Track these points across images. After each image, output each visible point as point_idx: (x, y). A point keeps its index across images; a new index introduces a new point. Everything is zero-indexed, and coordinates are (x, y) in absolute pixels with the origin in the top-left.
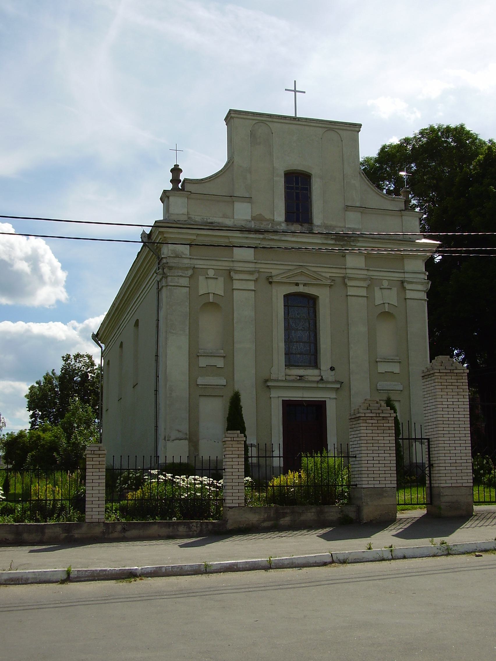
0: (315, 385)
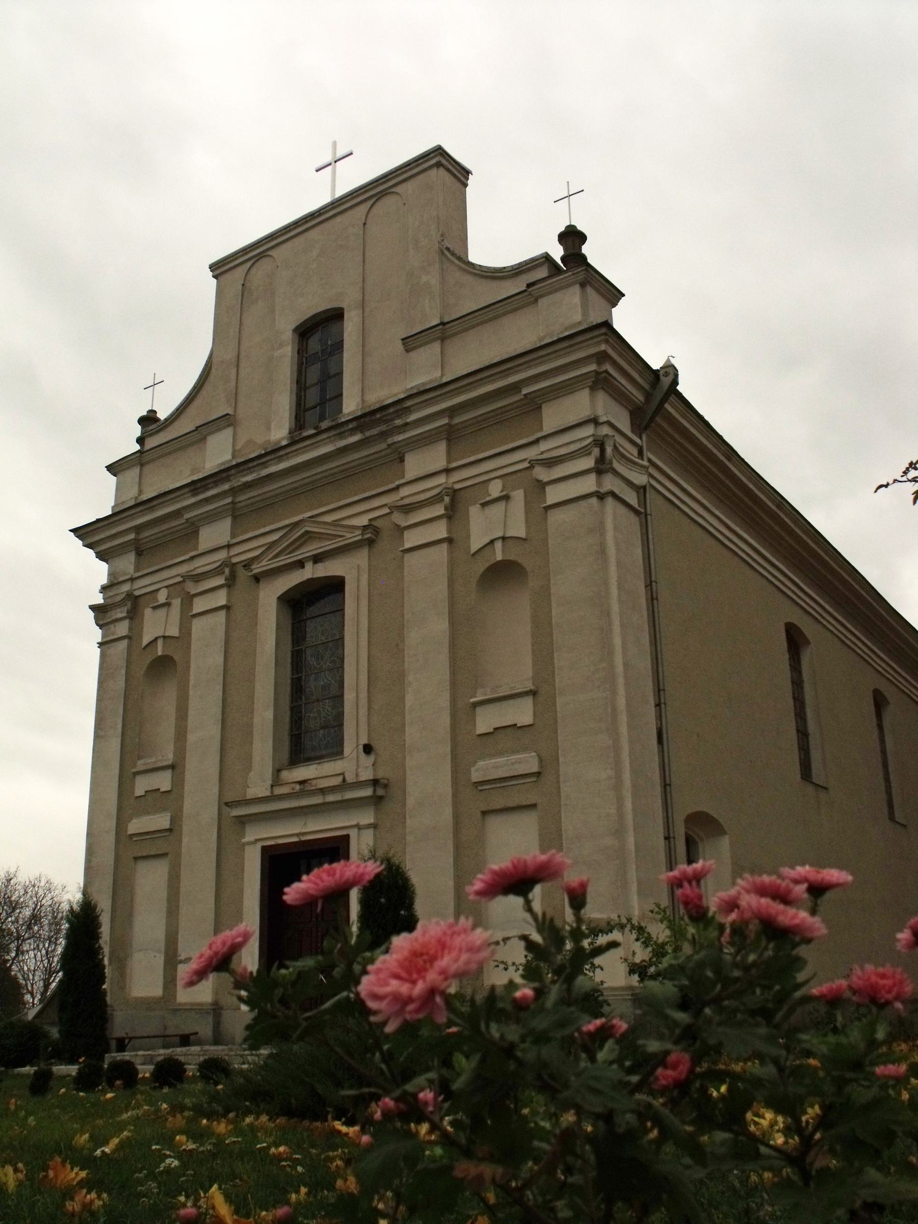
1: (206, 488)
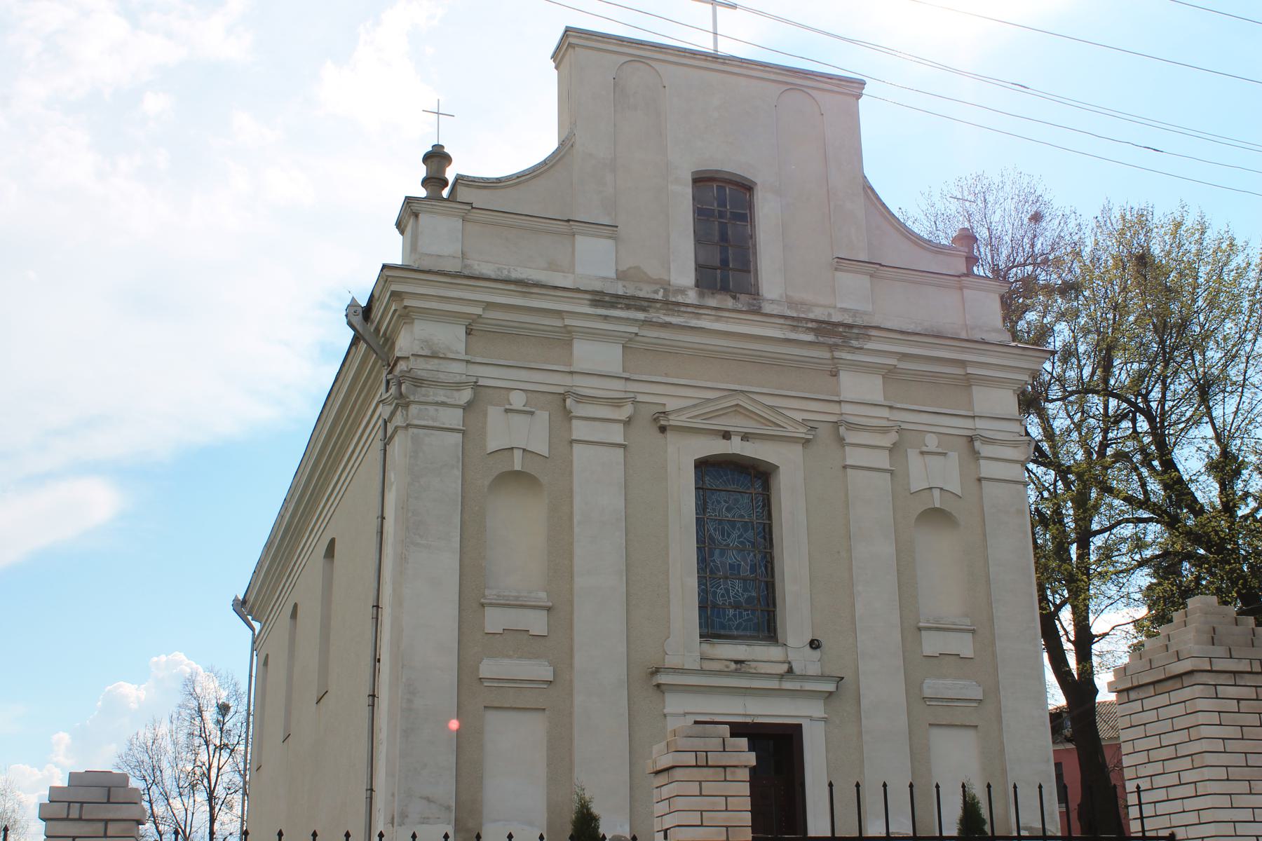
0: (774, 684)
1: (613, 306)
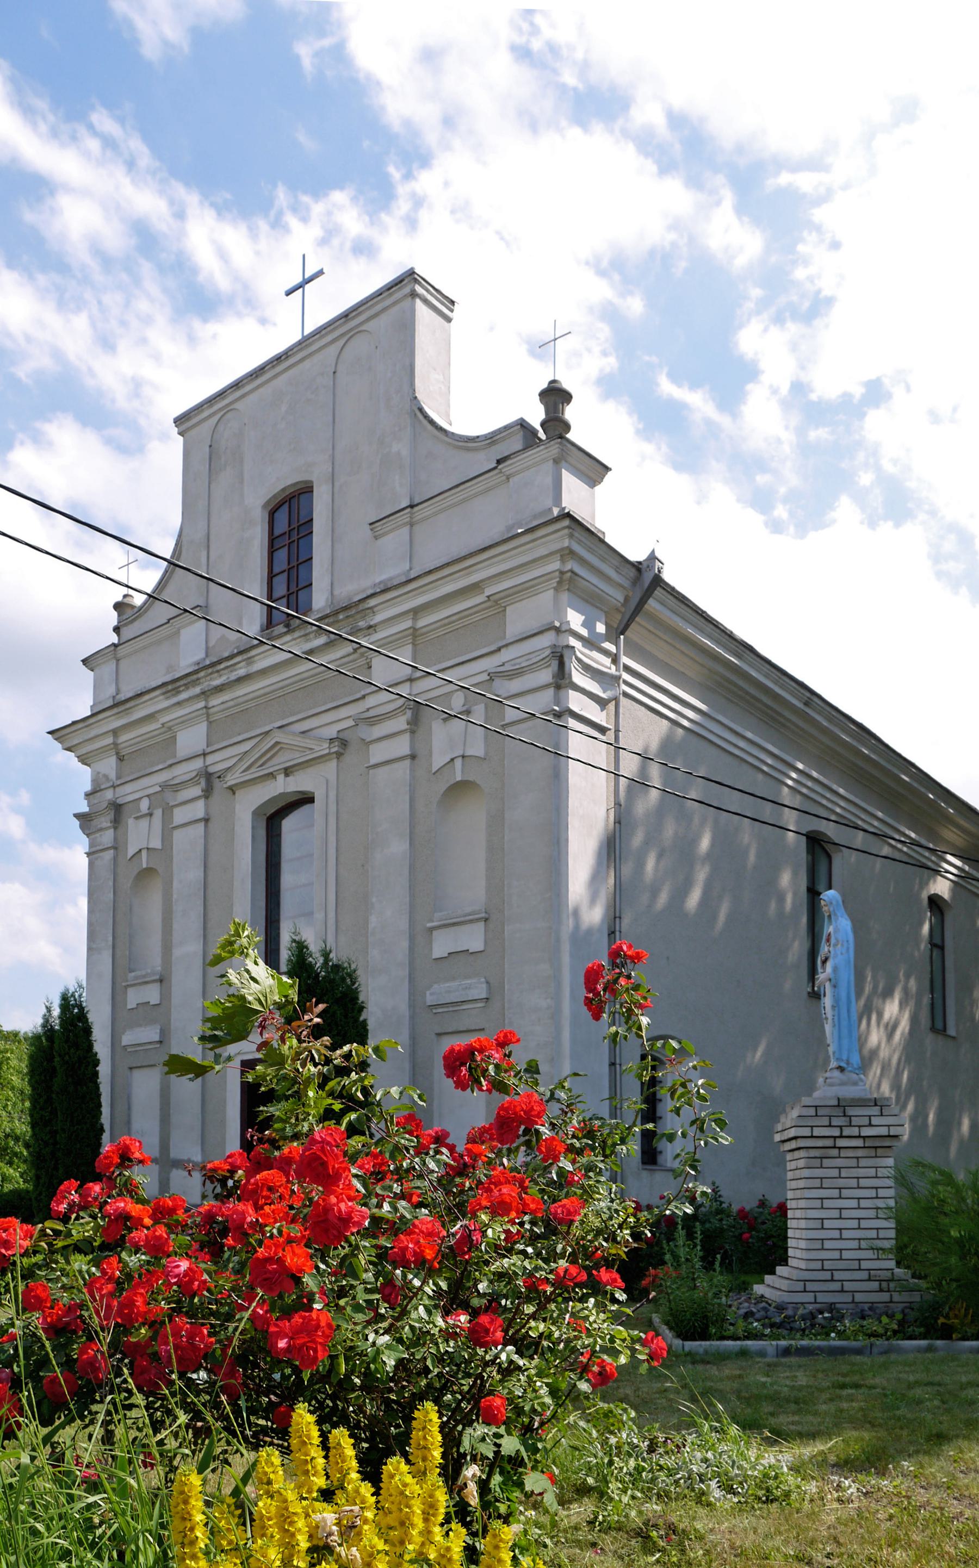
1: (177, 691)
